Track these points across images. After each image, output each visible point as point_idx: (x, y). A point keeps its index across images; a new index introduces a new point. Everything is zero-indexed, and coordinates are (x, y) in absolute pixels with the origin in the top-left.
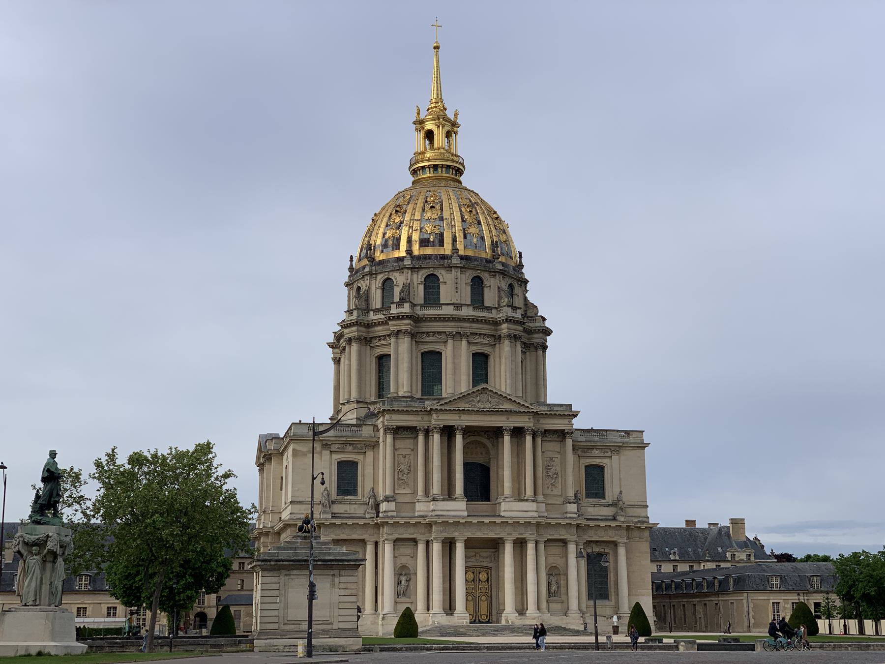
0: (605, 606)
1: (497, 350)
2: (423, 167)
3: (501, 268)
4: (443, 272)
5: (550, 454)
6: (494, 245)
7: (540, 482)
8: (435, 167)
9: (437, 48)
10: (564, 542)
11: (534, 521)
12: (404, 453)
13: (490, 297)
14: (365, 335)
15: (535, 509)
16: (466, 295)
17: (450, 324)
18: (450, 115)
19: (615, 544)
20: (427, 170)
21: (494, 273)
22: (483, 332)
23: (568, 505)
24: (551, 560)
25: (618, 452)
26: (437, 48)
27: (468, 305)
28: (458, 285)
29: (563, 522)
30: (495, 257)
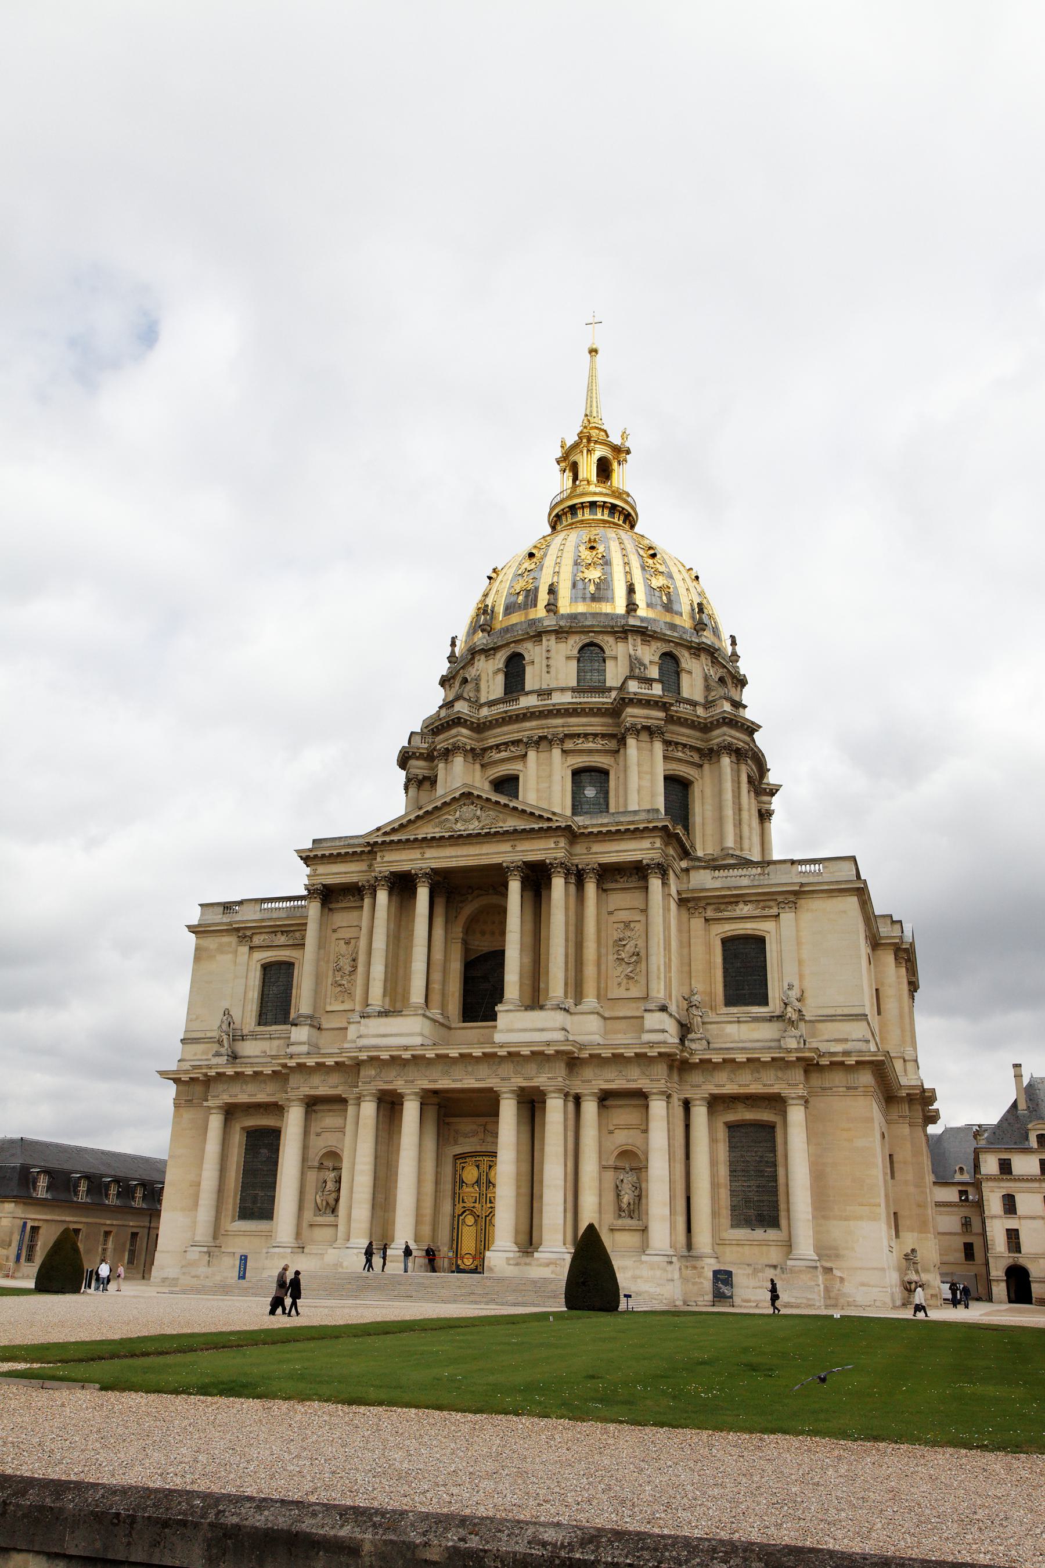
0: (765, 1243)
1: (622, 758)
2: (557, 516)
3: (638, 623)
4: (529, 645)
5: (624, 916)
6: (631, 590)
7: (590, 971)
8: (573, 509)
9: (593, 351)
10: (640, 1097)
11: (550, 1051)
12: (348, 936)
13: (614, 674)
14: (426, 773)
15: (558, 1025)
16: (566, 673)
17: (528, 724)
18: (615, 439)
19: (777, 1102)
20: (564, 518)
21: (623, 632)
22: (590, 730)
23: (647, 1015)
24: (622, 1138)
25: (794, 906)
26: (593, 351)
27: (563, 690)
28: (551, 662)
29: (629, 1053)
30: (631, 607)
